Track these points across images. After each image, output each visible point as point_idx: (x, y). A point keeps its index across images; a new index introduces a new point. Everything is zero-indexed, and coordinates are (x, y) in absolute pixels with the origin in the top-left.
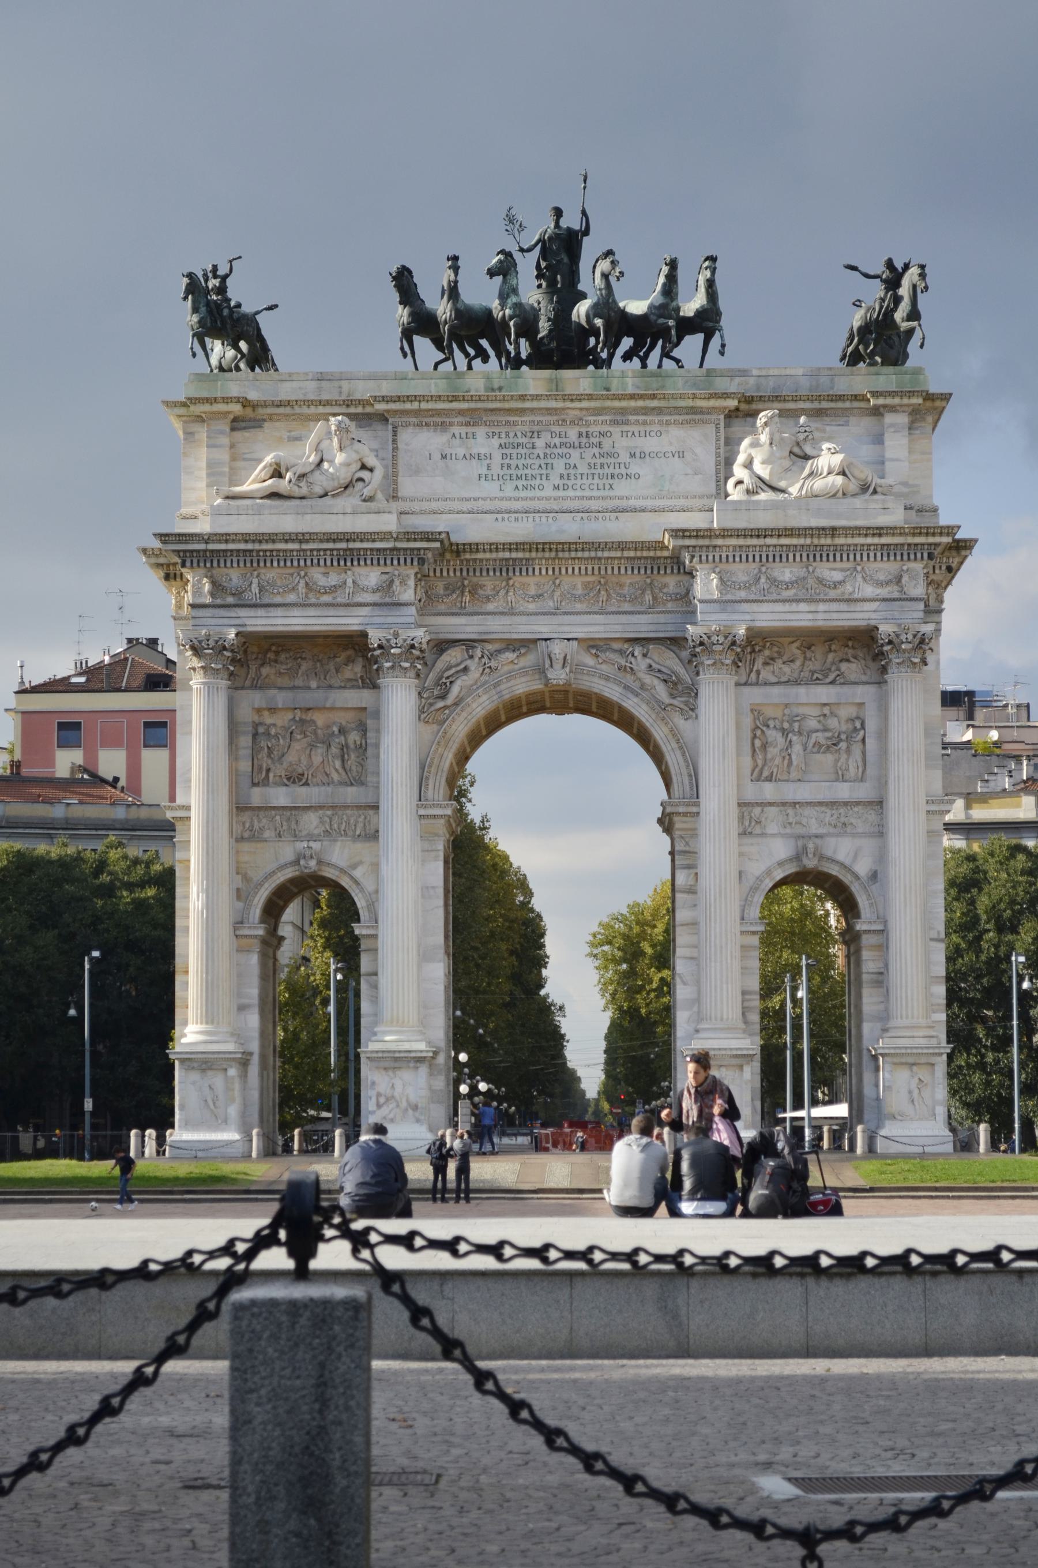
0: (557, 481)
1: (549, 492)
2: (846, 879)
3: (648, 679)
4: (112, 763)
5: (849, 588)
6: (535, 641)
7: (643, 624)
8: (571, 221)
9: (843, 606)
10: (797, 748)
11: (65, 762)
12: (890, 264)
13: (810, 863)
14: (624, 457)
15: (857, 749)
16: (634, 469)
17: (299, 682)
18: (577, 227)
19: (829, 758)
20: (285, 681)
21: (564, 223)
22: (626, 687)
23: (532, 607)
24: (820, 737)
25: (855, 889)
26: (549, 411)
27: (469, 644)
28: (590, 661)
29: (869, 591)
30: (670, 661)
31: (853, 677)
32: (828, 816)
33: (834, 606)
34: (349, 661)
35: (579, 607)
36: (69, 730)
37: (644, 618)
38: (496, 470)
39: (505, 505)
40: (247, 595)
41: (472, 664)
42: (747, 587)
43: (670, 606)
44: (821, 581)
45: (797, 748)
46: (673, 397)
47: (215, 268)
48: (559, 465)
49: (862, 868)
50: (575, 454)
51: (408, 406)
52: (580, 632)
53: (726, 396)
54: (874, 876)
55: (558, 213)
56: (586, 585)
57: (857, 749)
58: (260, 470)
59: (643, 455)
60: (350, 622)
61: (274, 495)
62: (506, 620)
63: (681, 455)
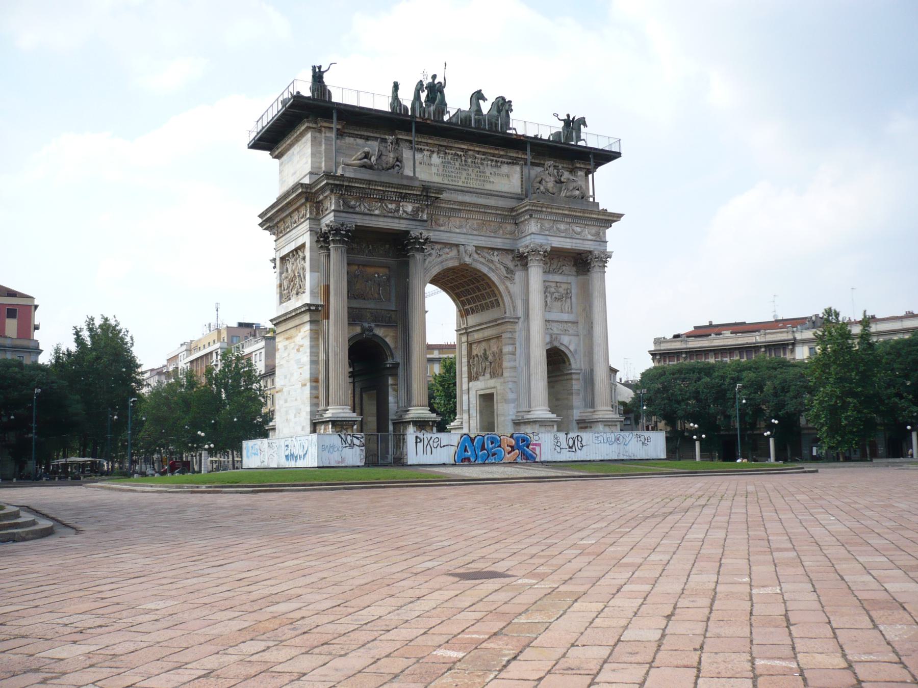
0: (463, 179)
1: (460, 184)
2: (567, 352)
3: (498, 266)
5: (583, 234)
6: (457, 245)
7: (498, 243)
9: (581, 241)
10: (549, 298)
12: (568, 116)
13: (556, 344)
14: (488, 174)
15: (569, 300)
16: (491, 180)
19: (559, 303)
22: (490, 268)
23: (458, 230)
24: (556, 295)
25: (570, 355)
26: (462, 150)
28: (476, 256)
29: (590, 237)
31: (566, 272)
32: (560, 326)
33: (578, 241)
35: (475, 232)
37: (499, 240)
38: (441, 172)
40: (357, 209)
41: (433, 252)
42: (549, 230)
43: (508, 236)
44: (573, 230)
47: (320, 67)
49: (572, 348)
50: (470, 169)
52: (476, 243)
54: (576, 350)
55: (434, 77)
56: (478, 224)
57: (569, 300)
58: (360, 154)
59: (495, 174)
60: (400, 225)
61: (363, 166)
62: (448, 235)
63: (508, 176)
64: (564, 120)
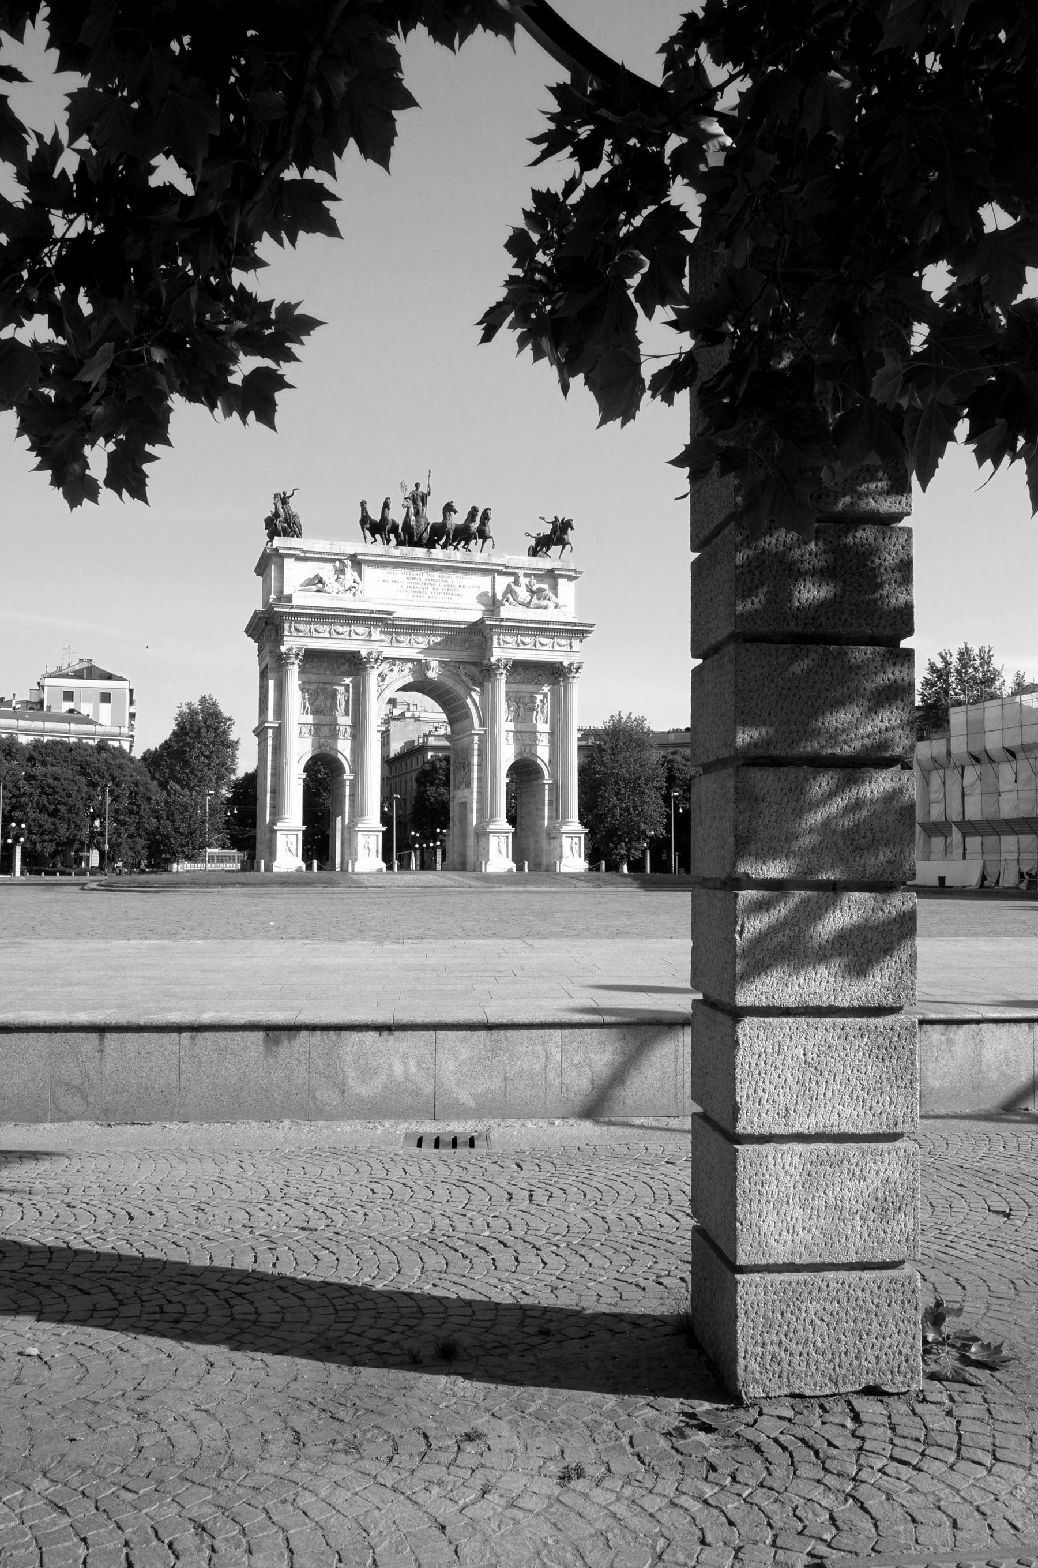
3: (465, 678)
4: (86, 709)
8: (423, 489)
10: (522, 709)
11: (68, 705)
12: (556, 518)
17: (321, 671)
18: (426, 492)
20: (315, 670)
21: (420, 489)
27: (395, 659)
30: (475, 671)
34: (343, 664)
36: (69, 696)
37: (465, 653)
38: (405, 588)
39: (409, 603)
45: (522, 709)
46: (476, 563)
47: (284, 493)
48: (431, 588)
51: (371, 558)
53: (501, 565)
55: (417, 485)
64: (552, 523)
